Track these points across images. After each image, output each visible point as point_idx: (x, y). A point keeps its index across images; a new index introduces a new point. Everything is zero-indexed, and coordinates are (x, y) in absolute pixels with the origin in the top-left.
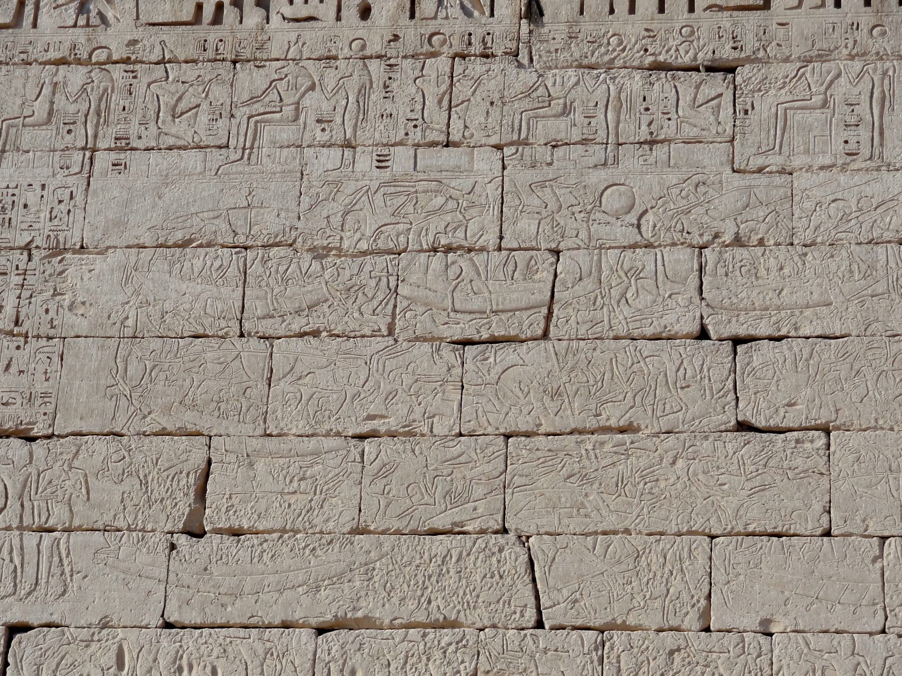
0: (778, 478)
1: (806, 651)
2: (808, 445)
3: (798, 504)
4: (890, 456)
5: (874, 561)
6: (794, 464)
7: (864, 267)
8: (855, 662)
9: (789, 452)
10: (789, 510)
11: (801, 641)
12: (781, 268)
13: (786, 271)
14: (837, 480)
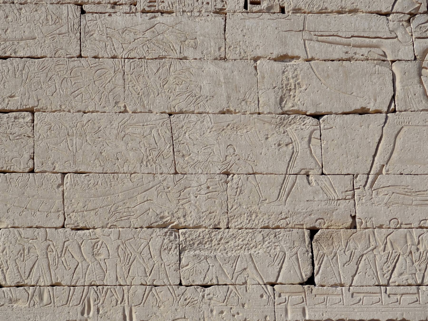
0: (4, 139)
1: (19, 238)
2: (21, 120)
3: (16, 154)
4: (68, 127)
5: (59, 186)
6: (13, 131)
7: (54, 17)
8: (47, 244)
9: (10, 124)
10: (10, 158)
11: (16, 233)
12: (7, 17)
13: (10, 18)
14: (37, 141)
